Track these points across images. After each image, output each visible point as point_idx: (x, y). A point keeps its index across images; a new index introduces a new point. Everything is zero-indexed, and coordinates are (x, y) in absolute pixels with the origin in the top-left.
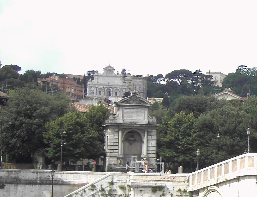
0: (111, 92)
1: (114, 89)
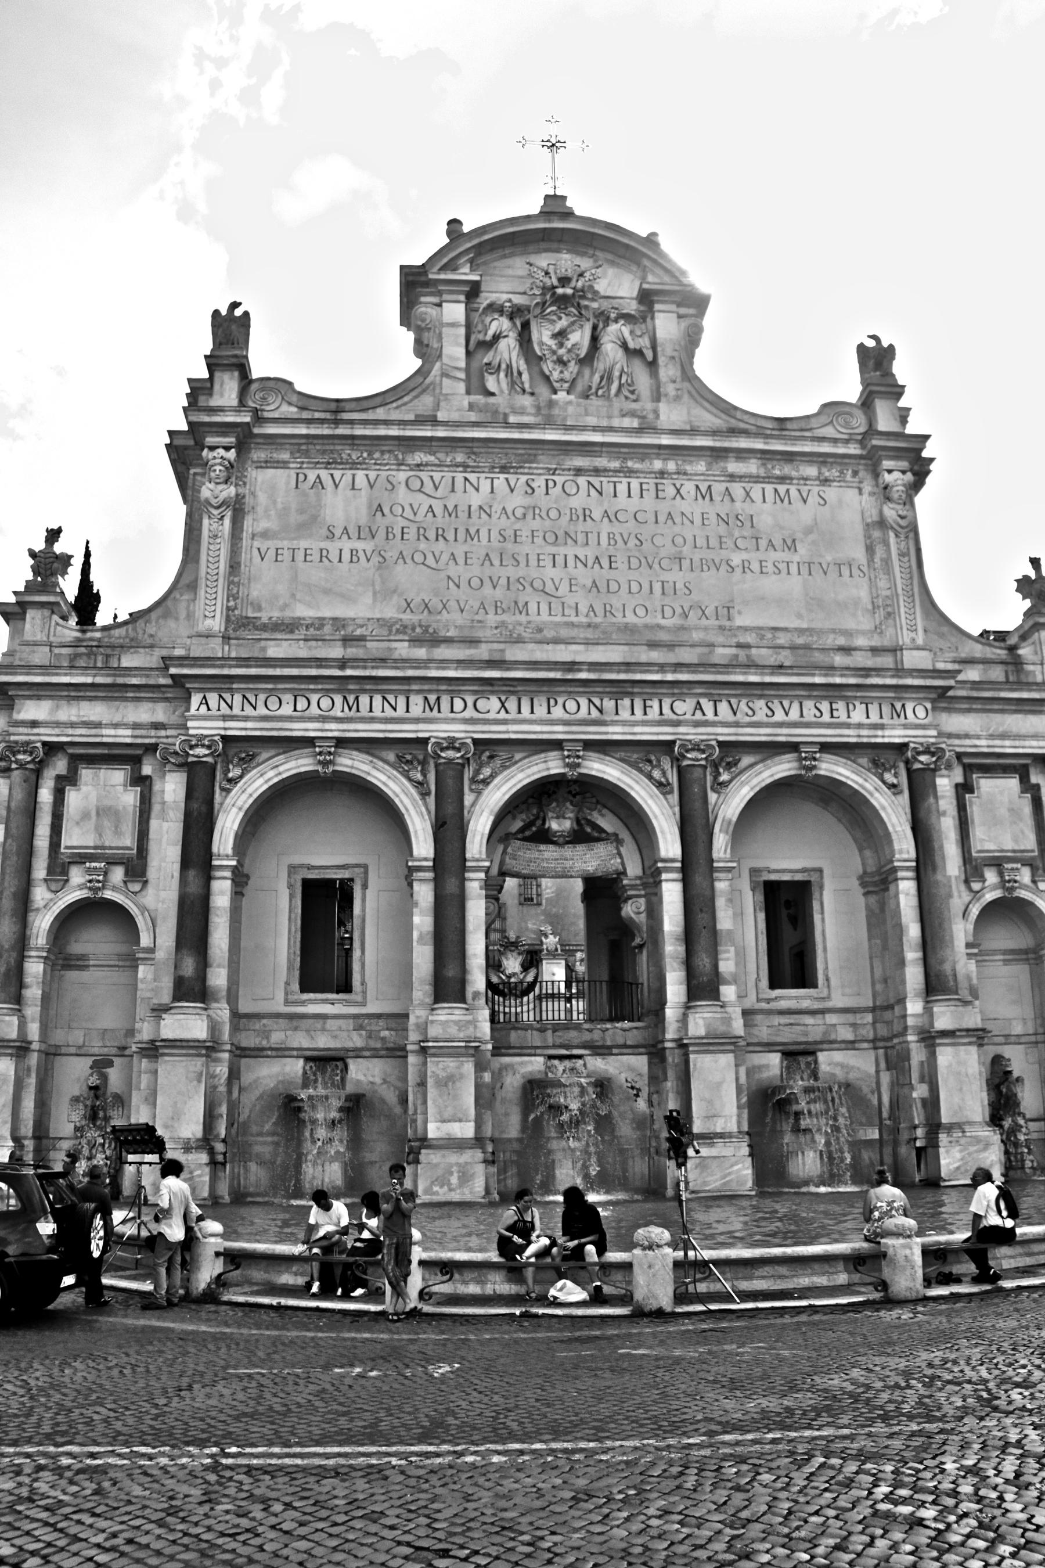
1: (730, 804)
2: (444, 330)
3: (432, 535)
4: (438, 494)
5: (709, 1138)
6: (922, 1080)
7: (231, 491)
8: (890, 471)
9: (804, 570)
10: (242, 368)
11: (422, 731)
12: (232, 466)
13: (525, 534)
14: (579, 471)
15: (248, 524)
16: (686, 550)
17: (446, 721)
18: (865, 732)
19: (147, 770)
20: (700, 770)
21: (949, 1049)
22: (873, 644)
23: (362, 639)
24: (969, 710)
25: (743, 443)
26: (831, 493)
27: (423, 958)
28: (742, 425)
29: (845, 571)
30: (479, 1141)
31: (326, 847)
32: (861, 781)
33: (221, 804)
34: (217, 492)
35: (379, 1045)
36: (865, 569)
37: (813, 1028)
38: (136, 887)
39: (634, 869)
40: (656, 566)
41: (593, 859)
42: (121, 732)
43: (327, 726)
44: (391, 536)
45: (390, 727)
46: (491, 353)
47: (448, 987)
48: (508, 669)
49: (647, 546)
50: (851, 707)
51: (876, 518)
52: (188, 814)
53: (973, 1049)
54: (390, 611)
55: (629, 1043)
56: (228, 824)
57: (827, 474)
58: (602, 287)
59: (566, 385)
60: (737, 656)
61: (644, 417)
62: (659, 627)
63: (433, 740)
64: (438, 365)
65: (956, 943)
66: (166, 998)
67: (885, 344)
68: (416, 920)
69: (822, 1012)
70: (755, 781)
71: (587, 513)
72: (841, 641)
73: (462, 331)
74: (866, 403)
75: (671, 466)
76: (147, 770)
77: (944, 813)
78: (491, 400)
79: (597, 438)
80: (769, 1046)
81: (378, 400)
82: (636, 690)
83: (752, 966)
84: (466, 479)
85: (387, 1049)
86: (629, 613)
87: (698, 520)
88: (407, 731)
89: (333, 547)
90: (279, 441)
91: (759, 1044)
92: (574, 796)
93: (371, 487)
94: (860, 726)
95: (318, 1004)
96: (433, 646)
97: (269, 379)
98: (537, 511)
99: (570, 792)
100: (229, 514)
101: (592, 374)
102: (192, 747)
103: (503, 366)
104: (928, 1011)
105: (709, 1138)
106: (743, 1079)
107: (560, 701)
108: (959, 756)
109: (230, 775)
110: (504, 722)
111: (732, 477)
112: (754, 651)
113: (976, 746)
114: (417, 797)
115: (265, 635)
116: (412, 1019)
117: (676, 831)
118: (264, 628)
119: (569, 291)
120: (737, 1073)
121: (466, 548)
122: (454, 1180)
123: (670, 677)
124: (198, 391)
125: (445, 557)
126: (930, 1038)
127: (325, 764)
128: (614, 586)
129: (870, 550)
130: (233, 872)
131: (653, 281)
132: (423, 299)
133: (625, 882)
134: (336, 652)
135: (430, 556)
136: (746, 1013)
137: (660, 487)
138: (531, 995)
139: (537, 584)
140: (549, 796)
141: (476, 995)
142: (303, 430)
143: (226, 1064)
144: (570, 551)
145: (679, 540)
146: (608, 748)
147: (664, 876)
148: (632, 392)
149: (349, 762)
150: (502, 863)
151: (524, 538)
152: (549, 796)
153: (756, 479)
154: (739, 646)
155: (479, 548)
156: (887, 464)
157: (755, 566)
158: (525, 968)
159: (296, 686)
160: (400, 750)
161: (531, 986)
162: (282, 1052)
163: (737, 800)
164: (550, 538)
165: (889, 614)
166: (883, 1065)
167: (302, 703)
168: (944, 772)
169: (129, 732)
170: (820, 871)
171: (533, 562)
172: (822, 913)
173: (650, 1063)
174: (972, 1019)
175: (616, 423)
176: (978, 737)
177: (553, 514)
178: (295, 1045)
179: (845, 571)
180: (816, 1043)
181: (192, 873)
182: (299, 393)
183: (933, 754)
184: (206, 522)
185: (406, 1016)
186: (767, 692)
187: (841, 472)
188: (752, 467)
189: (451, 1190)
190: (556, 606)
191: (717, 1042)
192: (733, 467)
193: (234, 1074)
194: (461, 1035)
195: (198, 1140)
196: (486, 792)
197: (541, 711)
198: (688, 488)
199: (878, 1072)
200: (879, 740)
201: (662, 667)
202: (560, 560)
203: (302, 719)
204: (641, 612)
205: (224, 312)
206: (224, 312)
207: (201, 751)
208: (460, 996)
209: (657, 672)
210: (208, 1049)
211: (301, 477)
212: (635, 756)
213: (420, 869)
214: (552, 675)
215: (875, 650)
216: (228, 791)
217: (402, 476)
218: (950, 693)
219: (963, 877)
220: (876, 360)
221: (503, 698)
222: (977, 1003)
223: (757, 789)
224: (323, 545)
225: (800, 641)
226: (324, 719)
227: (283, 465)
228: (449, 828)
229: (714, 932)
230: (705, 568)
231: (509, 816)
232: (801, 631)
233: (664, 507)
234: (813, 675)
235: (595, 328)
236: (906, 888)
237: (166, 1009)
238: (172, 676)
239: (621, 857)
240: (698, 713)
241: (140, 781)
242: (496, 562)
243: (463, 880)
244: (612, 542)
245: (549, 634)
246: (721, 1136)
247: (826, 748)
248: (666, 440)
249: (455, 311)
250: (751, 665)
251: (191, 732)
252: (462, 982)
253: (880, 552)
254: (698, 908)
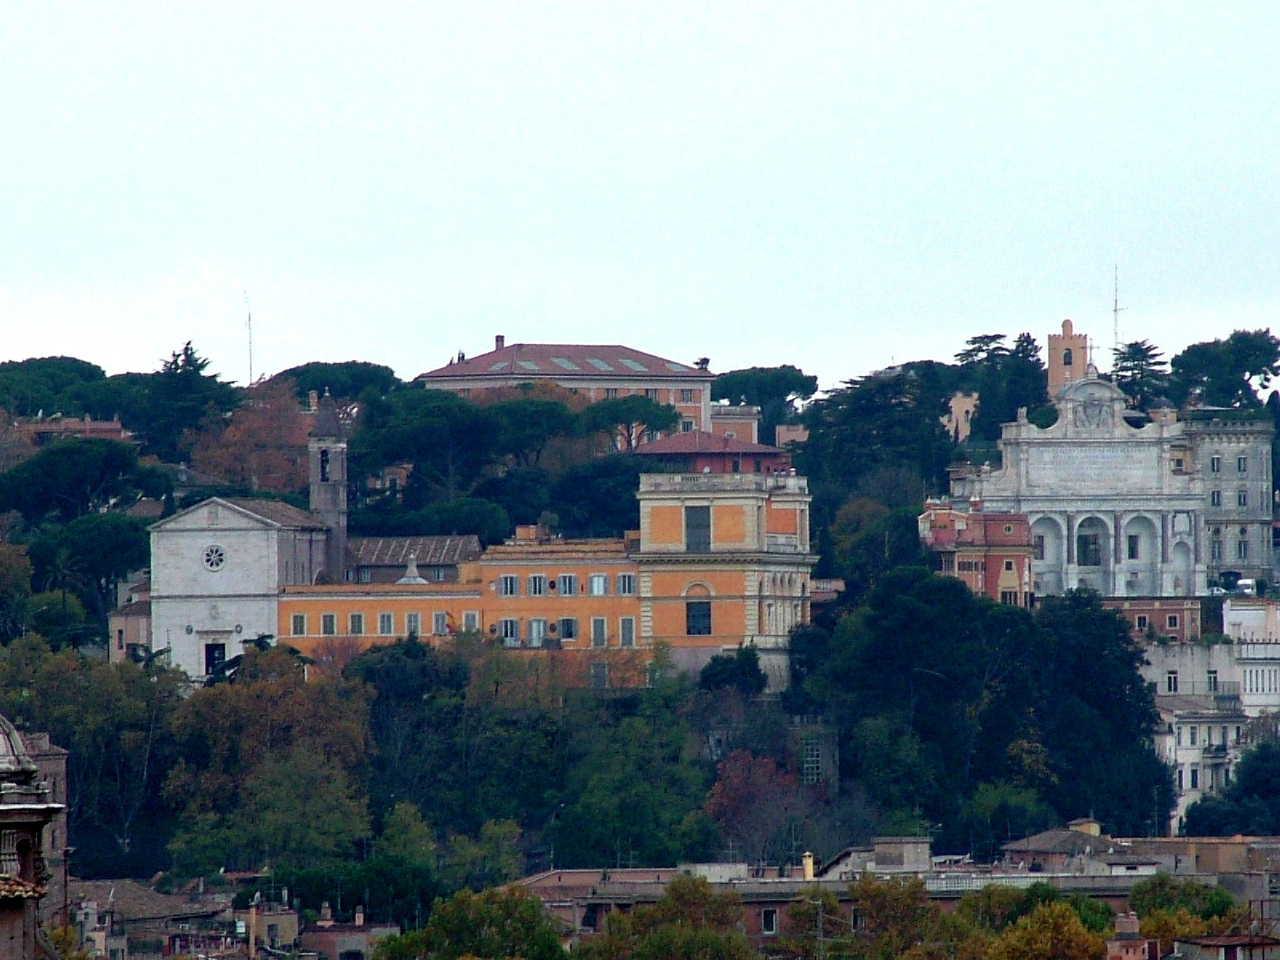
27: (1065, 555)
47: (1069, 561)
155: (1075, 466)
228: (1070, 528)
254: (1117, 544)
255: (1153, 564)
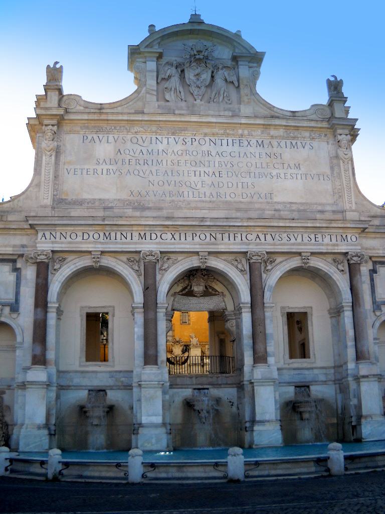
0: (231, 325)
2: (147, 74)
3: (142, 162)
4: (145, 145)
5: (262, 422)
6: (355, 397)
7: (56, 143)
8: (341, 135)
9: (304, 177)
10: (60, 91)
11: (138, 248)
12: (55, 133)
13: (183, 161)
14: (206, 135)
15: (62, 158)
16: (253, 169)
17: (148, 243)
18: (330, 247)
19: (19, 265)
20: (259, 264)
21: (366, 384)
22: (334, 209)
23: (112, 208)
24: (375, 238)
25: (277, 122)
26: (315, 144)
27: (139, 346)
28: (277, 114)
29: (321, 178)
30: (164, 424)
31: (96, 297)
32: (328, 268)
33: (51, 280)
34: (49, 144)
35: (120, 384)
36: (330, 177)
37: (308, 376)
38: (14, 316)
39: (230, 307)
40: (239, 176)
41: (212, 303)
42: (7, 249)
43: (97, 246)
44: (124, 163)
45: (124, 246)
46: (168, 83)
47: (150, 358)
48: (175, 221)
49: (235, 167)
50: (324, 236)
51: (334, 155)
52: (37, 284)
53: (376, 384)
54: (124, 196)
55: (229, 382)
56: (55, 288)
57: (313, 136)
58: (216, 54)
59: (200, 97)
60: (274, 215)
61: (234, 111)
62: (241, 202)
63: (143, 252)
64: (144, 88)
65: (369, 338)
66: (28, 362)
67: (339, 79)
68: (136, 330)
69: (312, 368)
70: (282, 269)
71: (209, 152)
72: (320, 208)
73: (155, 74)
74: (331, 104)
75: (246, 132)
76: (19, 265)
77: (364, 282)
78: (167, 104)
79: (214, 120)
80: (289, 384)
81: (119, 104)
82: (231, 230)
83: (282, 348)
84: (156, 138)
85: (124, 386)
86: (228, 196)
87: (257, 156)
88: (132, 248)
89: (99, 168)
90: (76, 122)
91: (284, 383)
92: (204, 276)
93: (116, 142)
94: (328, 245)
95: (93, 367)
96: (142, 211)
97: (71, 95)
98: (188, 152)
99: (202, 274)
100: (54, 154)
101: (212, 93)
102: (38, 255)
103: (173, 89)
104: (357, 367)
105: (262, 422)
106: (277, 398)
107: (198, 235)
108: (370, 258)
109: (55, 267)
110: (174, 244)
111: (272, 137)
112: (282, 212)
113: (378, 253)
114: (136, 277)
115: (70, 207)
116: (135, 372)
117: (249, 292)
118: (69, 203)
119: (202, 57)
120: (275, 395)
121: (157, 168)
122: (154, 441)
123: (245, 224)
124: (39, 100)
125: (147, 172)
126: (357, 379)
127: (96, 262)
128: (221, 185)
129: (332, 168)
130: (57, 310)
131: (238, 52)
132: (138, 60)
133: (226, 313)
134: (101, 213)
135: (141, 172)
136: (279, 369)
137: (241, 141)
138: (186, 364)
139: (188, 183)
140: (193, 276)
141: (162, 362)
142: (86, 117)
143: (55, 392)
144: (202, 169)
145: (249, 165)
146: (218, 255)
147: (243, 310)
148: (229, 100)
149: (106, 262)
150: (173, 305)
151: (182, 164)
152: (193, 276)
153: (283, 138)
154: (275, 210)
156: (339, 131)
157: (282, 176)
158: (184, 352)
159: (83, 228)
160: (129, 256)
161: (186, 361)
162: (78, 387)
163: (275, 277)
164: (194, 164)
165: (340, 196)
166: (338, 391)
167: (86, 236)
168: (364, 264)
169: (11, 249)
170: (311, 308)
171: (186, 174)
172: (312, 326)
173: (238, 391)
174: (375, 370)
175: (222, 113)
176: (379, 249)
177: (195, 153)
178: (84, 384)
179: (321, 178)
180: (310, 382)
181: (39, 310)
182: (84, 101)
183: (359, 257)
184: (44, 158)
185: (132, 371)
186: (287, 230)
187: (320, 135)
188: (281, 132)
189: (152, 445)
190: (196, 193)
191: (266, 381)
192: (273, 132)
193: (58, 397)
194: (156, 379)
195: (44, 424)
196: (166, 274)
197: (189, 239)
198: (253, 142)
199: (336, 394)
200: (336, 251)
201: (242, 219)
202: (198, 173)
203: (86, 243)
204: (233, 195)
205: (52, 66)
206: (52, 66)
207: (42, 257)
208: (155, 363)
209: (240, 222)
210: (48, 385)
211: (85, 138)
212: (231, 258)
213: (137, 308)
214: (194, 223)
215: (334, 212)
216: (55, 274)
217: (129, 137)
218: (366, 230)
219: (372, 310)
220: (335, 87)
221: (173, 234)
222: (378, 364)
223: (283, 272)
224: (95, 167)
225: (302, 208)
226: (95, 243)
227: (78, 132)
228: (150, 290)
229: (265, 334)
230: (261, 176)
231: (176, 285)
232: (302, 204)
233: (242, 150)
234: (308, 223)
235: (213, 72)
236: (348, 315)
237: (29, 368)
238: (30, 225)
239: (225, 303)
240: (258, 239)
241: (16, 270)
242: (170, 174)
243: (156, 312)
244: (220, 165)
245: (193, 205)
246: (268, 421)
247: (313, 254)
248: (243, 121)
249: (152, 65)
250: (281, 218)
251: (38, 249)
252: (156, 357)
253: (336, 169)
254: (257, 324)
255: (339, 366)
